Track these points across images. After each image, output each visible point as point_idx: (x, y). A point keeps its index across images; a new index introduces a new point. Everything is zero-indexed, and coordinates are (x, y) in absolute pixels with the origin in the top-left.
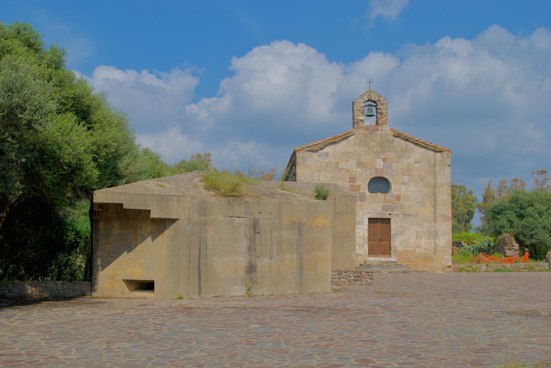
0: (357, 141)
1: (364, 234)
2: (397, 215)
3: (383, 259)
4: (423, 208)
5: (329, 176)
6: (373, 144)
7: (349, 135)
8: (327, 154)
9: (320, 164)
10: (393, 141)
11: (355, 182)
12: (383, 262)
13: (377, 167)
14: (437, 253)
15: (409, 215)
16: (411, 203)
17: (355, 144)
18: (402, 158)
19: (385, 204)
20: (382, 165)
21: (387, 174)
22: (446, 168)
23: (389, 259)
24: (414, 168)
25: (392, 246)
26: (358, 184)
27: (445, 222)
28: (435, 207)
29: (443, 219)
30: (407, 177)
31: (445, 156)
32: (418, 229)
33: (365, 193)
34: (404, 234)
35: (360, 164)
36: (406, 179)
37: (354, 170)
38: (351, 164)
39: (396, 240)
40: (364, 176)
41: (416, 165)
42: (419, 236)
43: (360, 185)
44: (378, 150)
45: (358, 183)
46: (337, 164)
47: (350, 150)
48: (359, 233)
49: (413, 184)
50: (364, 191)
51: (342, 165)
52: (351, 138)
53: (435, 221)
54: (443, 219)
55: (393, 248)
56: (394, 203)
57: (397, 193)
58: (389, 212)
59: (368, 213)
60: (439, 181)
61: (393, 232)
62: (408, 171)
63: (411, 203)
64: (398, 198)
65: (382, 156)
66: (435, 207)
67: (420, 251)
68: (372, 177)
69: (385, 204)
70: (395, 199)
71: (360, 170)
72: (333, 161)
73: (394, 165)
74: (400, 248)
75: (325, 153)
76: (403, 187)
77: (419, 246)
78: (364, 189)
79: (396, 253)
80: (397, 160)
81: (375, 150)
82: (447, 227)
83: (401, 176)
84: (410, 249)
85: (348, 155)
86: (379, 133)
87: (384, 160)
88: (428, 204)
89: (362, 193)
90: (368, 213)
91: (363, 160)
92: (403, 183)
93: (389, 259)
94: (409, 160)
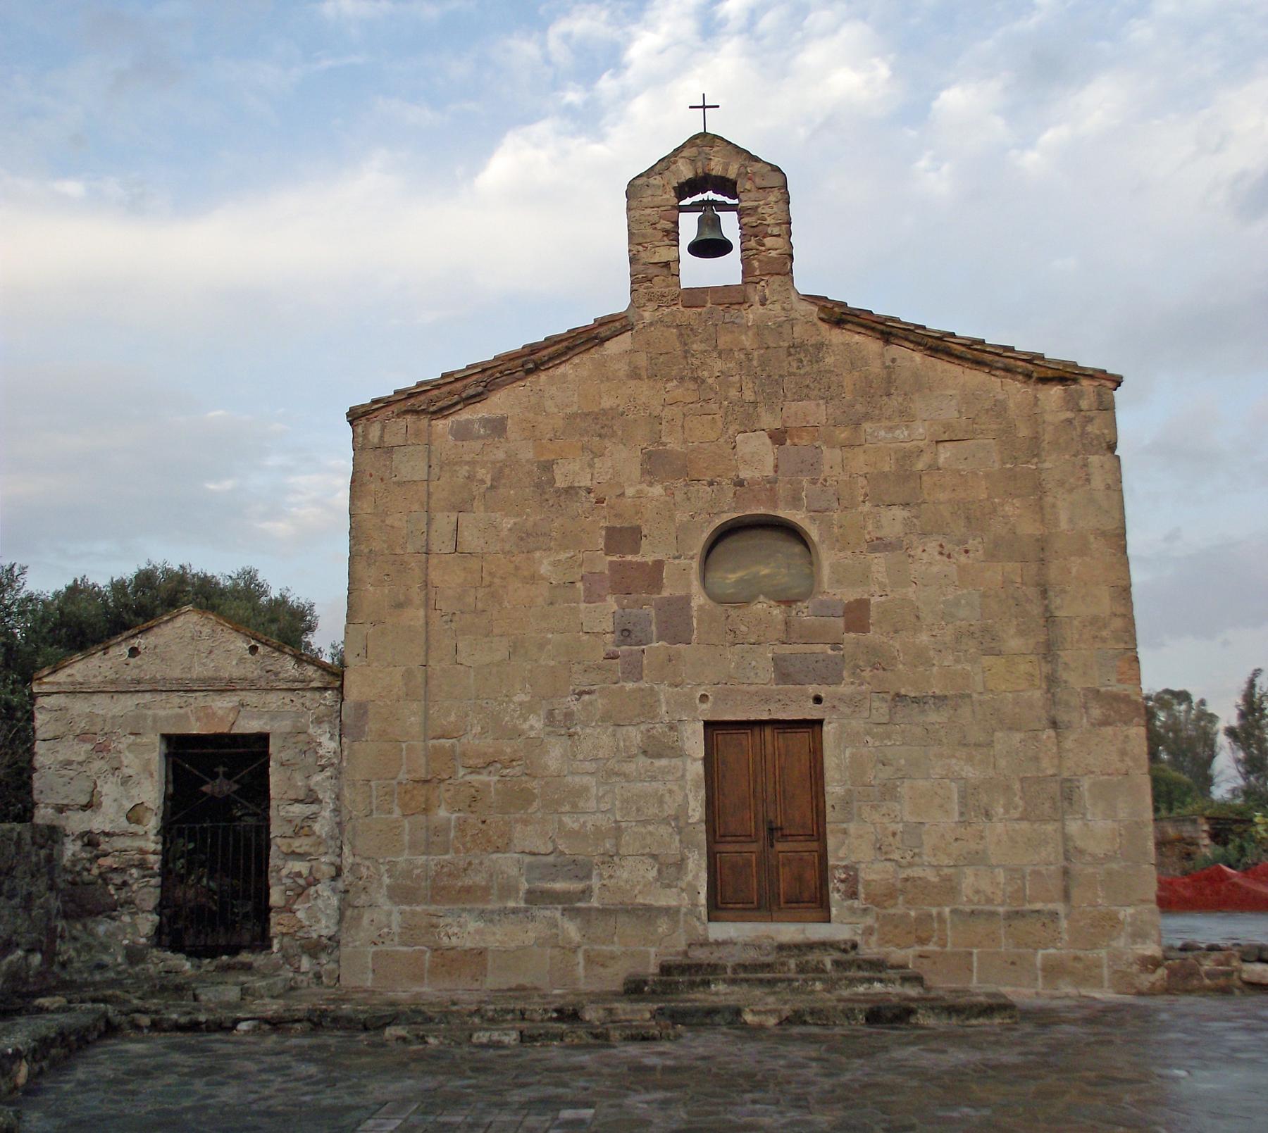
0: (642, 360)
1: (684, 807)
2: (854, 703)
3: (789, 932)
4: (987, 661)
5: (508, 523)
6: (719, 365)
7: (603, 332)
8: (498, 427)
9: (464, 471)
10: (820, 346)
11: (636, 551)
12: (781, 947)
13: (745, 474)
14: (1075, 893)
15: (915, 700)
16: (924, 638)
17: (635, 374)
18: (867, 426)
19: (786, 650)
20: (770, 461)
21: (795, 501)
22: (1094, 459)
23: (817, 931)
24: (934, 467)
25: (832, 861)
26: (650, 559)
27: (1109, 730)
28: (1049, 651)
29: (1096, 712)
30: (899, 513)
31: (1084, 404)
32: (970, 772)
33: (686, 600)
34: (896, 798)
35: (656, 464)
36: (893, 521)
37: (630, 491)
38: (621, 462)
39: (852, 827)
40: (681, 517)
41: (945, 454)
42: (973, 804)
43: (659, 564)
44: (749, 396)
45: (647, 555)
46: (548, 467)
47: (607, 403)
48: (661, 802)
49: (932, 547)
50: (680, 592)
51: (570, 472)
52: (612, 347)
53: (1054, 724)
54: (1096, 712)
55: (837, 877)
56: (836, 645)
57: (851, 595)
58: (812, 689)
59: (704, 698)
60: (1064, 525)
61: (834, 789)
62: (903, 482)
63: (924, 638)
64: (857, 616)
65: (770, 421)
66: (1049, 651)
67: (985, 885)
68: (718, 522)
69: (786, 650)
70: (841, 623)
71: (657, 490)
72: (527, 453)
73: (831, 456)
74: (874, 873)
75: (486, 422)
76: (879, 564)
77: (977, 859)
78: (684, 579)
79: (853, 895)
80: (843, 434)
81: (733, 393)
82: (1123, 753)
83: (867, 507)
84: (932, 877)
85: (599, 425)
86: (751, 315)
87: (778, 437)
88: (1014, 643)
89: (670, 601)
90: (704, 698)
91: (673, 443)
92: (879, 545)
93: (817, 931)
94: (901, 434)
